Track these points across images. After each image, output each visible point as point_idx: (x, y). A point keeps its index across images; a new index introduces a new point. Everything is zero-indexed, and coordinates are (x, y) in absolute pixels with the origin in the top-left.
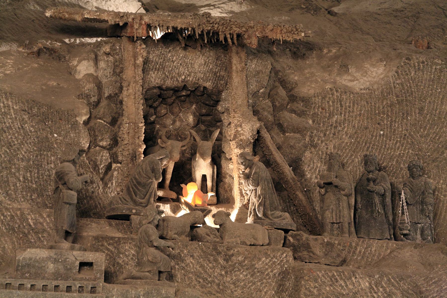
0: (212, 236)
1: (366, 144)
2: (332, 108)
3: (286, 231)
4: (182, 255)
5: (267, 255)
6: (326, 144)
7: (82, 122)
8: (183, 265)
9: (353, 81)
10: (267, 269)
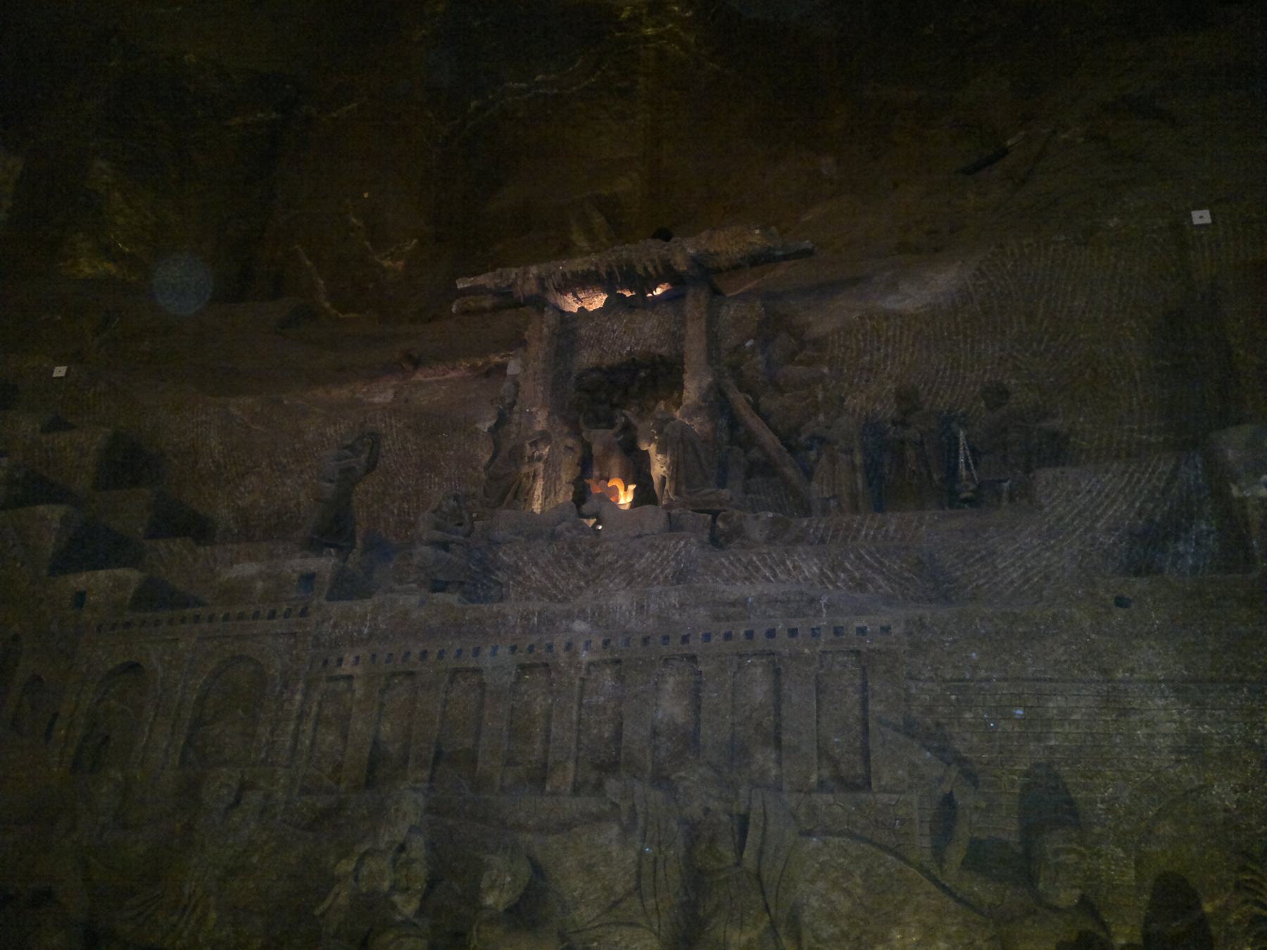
0: (575, 532)
1: (925, 385)
2: (862, 344)
3: (715, 514)
4: (520, 564)
5: (652, 547)
7: (486, 430)
8: (520, 578)
9: (904, 300)
10: (654, 570)
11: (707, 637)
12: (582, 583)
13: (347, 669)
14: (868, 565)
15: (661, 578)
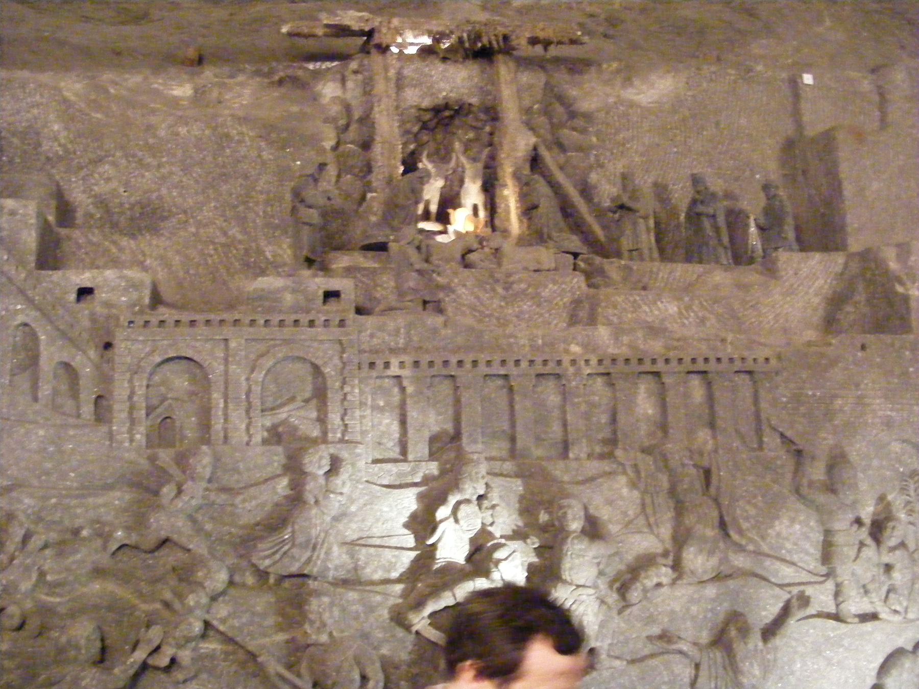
3: (576, 255)
5: (555, 282)
6: (614, 164)
10: (555, 298)
11: (667, 361)
12: (503, 304)
13: (394, 370)
14: (706, 309)
15: (561, 303)
